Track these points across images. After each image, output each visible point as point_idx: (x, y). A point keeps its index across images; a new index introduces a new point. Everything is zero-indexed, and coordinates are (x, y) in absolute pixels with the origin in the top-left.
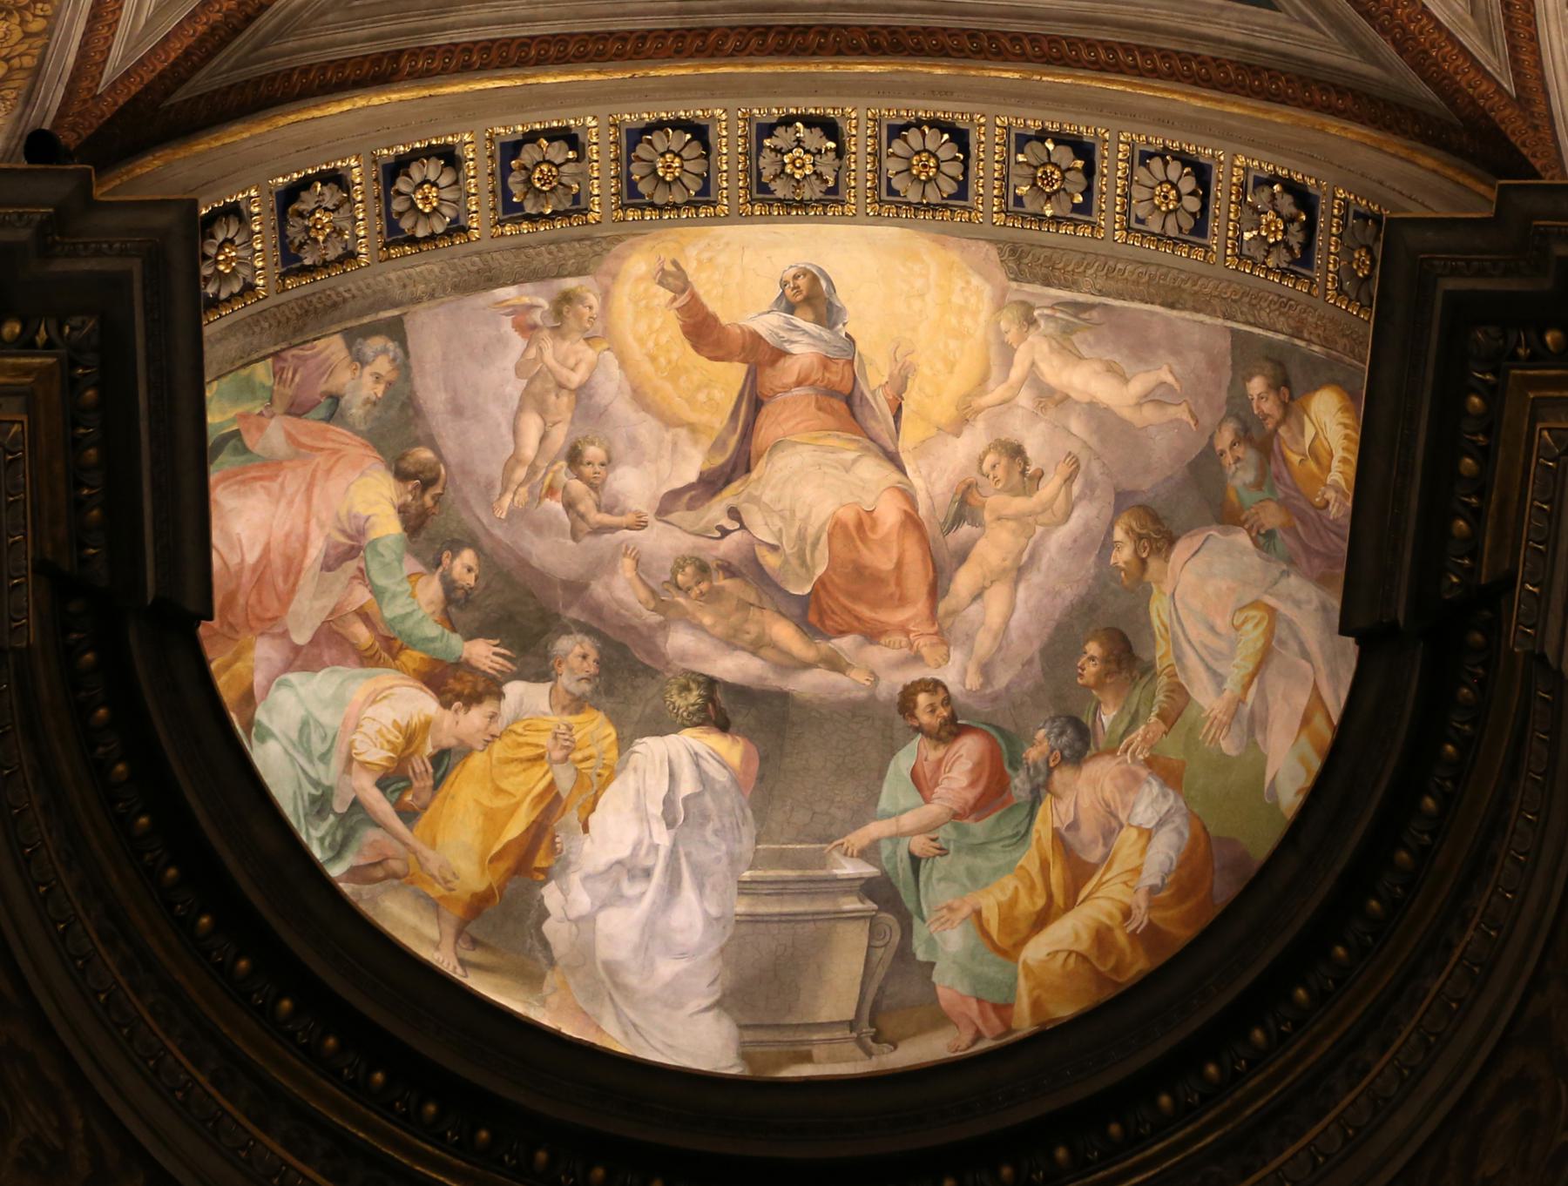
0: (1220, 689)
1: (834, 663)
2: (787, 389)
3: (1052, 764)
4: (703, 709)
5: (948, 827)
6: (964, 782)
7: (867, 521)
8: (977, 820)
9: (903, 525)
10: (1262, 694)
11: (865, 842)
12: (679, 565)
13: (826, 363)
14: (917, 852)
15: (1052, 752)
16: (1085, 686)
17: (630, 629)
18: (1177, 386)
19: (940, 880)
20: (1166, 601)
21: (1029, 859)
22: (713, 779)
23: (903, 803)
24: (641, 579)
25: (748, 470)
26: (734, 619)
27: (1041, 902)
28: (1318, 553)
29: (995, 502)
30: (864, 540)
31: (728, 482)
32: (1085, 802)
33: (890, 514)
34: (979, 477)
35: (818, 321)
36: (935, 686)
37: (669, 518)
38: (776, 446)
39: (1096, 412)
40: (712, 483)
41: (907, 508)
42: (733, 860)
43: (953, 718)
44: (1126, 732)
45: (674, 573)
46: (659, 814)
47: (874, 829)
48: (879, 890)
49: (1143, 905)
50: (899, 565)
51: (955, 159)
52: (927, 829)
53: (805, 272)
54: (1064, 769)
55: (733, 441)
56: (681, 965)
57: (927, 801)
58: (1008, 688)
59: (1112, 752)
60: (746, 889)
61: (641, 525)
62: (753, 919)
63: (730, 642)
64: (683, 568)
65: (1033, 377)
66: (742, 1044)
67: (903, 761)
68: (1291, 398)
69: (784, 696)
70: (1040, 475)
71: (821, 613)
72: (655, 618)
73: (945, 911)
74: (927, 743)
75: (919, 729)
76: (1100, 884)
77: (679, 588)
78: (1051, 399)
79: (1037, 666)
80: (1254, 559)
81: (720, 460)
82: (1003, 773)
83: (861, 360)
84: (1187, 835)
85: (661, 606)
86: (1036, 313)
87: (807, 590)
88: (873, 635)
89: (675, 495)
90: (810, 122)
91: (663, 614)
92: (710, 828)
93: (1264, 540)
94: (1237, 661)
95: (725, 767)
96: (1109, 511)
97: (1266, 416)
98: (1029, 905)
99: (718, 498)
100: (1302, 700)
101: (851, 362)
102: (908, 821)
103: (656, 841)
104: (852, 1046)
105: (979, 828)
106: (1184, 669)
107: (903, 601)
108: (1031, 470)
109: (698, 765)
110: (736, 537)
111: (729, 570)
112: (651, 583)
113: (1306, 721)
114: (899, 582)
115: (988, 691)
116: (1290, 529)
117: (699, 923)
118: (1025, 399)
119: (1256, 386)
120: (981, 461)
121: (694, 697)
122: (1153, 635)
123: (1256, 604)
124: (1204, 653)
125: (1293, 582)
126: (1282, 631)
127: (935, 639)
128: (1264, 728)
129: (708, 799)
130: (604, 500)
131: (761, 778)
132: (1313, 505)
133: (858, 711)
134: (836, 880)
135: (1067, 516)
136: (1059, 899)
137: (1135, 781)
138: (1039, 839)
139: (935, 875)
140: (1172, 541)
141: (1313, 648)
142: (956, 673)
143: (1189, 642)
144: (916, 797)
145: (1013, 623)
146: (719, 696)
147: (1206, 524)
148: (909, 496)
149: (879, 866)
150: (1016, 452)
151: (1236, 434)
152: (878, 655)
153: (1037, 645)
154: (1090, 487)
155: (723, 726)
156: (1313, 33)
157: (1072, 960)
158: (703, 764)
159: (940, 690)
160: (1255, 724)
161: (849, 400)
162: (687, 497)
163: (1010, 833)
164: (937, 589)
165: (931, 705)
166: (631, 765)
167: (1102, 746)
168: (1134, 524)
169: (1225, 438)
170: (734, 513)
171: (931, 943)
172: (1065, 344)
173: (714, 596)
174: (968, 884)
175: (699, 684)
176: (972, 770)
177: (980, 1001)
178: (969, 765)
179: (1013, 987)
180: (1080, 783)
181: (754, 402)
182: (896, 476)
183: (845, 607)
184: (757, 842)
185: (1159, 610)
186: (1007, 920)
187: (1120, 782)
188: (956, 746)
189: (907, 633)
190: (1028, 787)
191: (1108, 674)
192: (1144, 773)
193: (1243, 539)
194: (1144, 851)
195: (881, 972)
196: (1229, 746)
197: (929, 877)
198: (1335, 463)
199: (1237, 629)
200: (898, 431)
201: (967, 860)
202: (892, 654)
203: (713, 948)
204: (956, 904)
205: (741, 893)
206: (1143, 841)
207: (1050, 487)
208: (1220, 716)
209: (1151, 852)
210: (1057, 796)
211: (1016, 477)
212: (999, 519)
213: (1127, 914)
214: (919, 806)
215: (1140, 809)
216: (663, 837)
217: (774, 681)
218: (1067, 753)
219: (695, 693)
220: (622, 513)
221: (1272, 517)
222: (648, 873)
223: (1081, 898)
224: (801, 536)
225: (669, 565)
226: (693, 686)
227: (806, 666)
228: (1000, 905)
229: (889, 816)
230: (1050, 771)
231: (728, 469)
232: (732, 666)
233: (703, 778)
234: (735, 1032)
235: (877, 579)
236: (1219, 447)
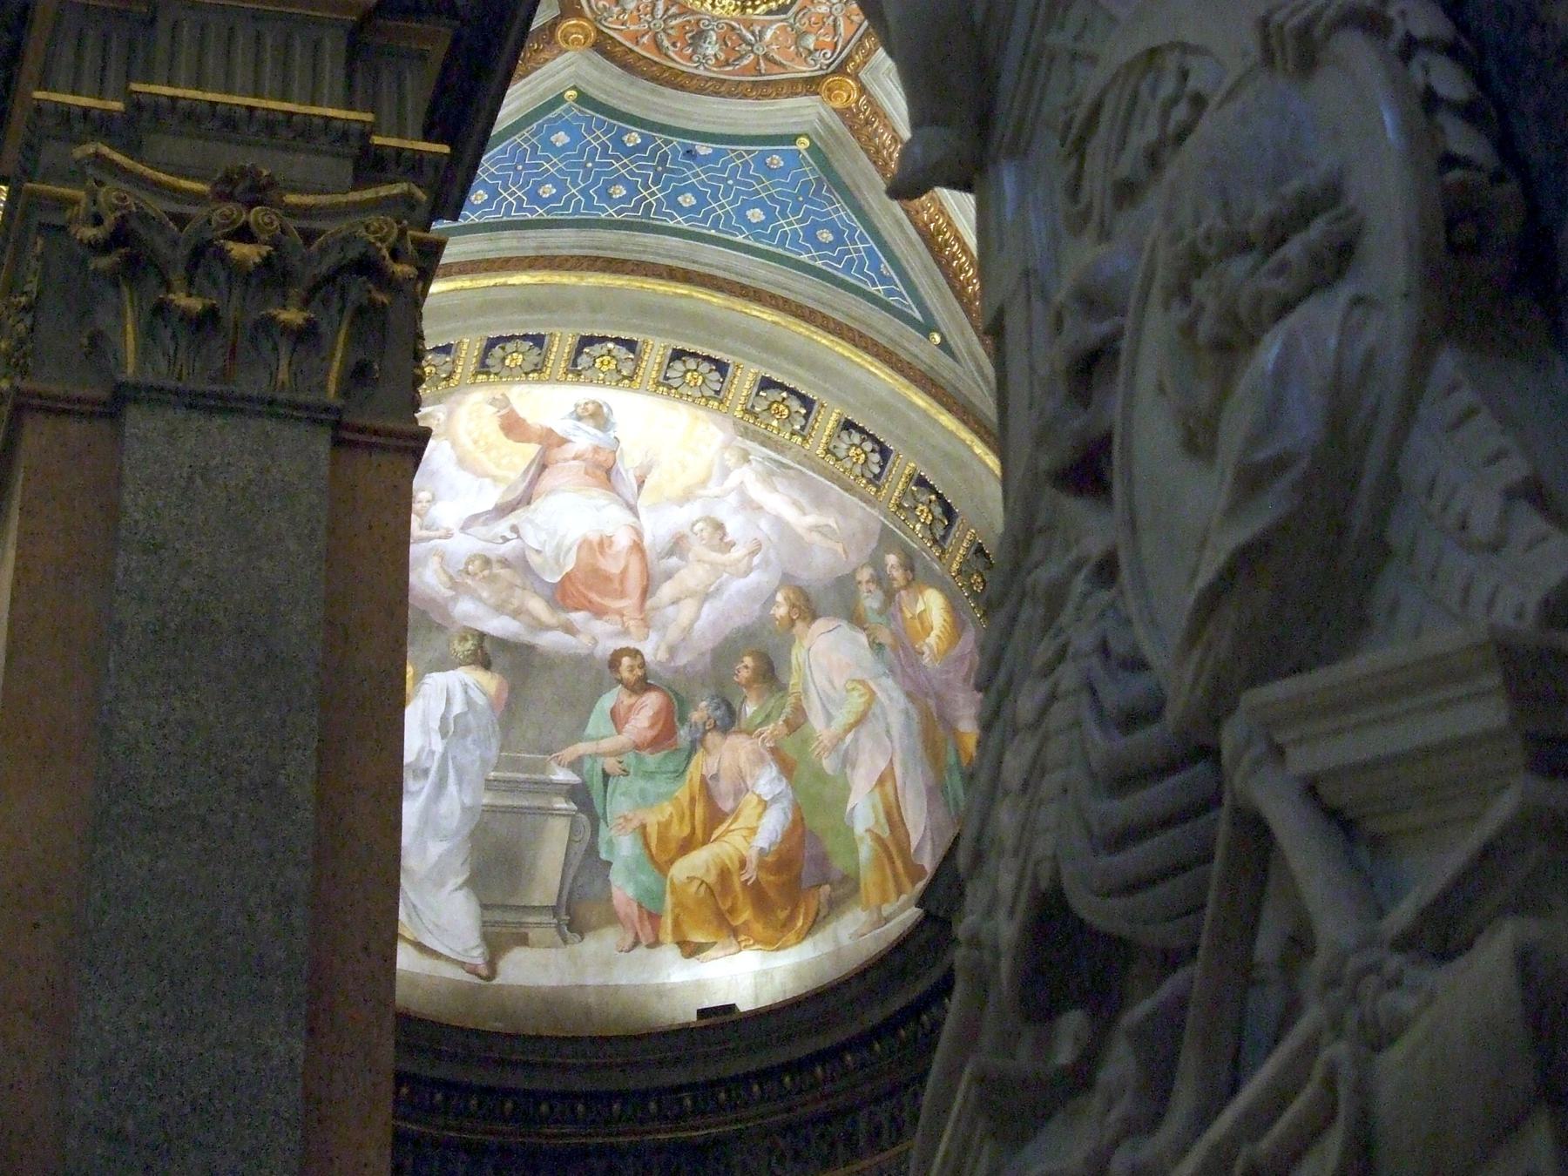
0: (828, 725)
1: (569, 629)
2: (566, 460)
3: (707, 728)
4: (474, 653)
5: (631, 755)
6: (646, 724)
7: (606, 543)
8: (652, 754)
9: (631, 548)
10: (856, 740)
11: (574, 757)
12: (470, 561)
13: (596, 449)
14: (608, 770)
15: (709, 718)
16: (739, 683)
17: (432, 600)
18: (838, 531)
19: (623, 794)
20: (803, 652)
21: (683, 792)
22: (475, 702)
23: (603, 731)
24: (444, 570)
25: (529, 503)
26: (504, 595)
27: (686, 831)
28: (909, 677)
29: (697, 549)
30: (602, 552)
31: (514, 510)
32: (726, 763)
33: (623, 540)
34: (690, 534)
35: (598, 427)
36: (635, 653)
37: (469, 531)
38: (552, 491)
39: (778, 521)
40: (503, 510)
41: (636, 538)
42: (484, 762)
43: (644, 678)
44: (761, 724)
45: (467, 564)
46: (437, 728)
47: (582, 748)
48: (579, 795)
49: (755, 862)
50: (624, 572)
51: (711, 370)
52: (617, 753)
53: (594, 402)
54: (715, 733)
55: (522, 486)
56: (445, 845)
57: (619, 732)
58: (685, 667)
59: (750, 734)
60: (490, 785)
61: (448, 535)
62: (492, 809)
63: (499, 609)
64: (473, 561)
65: (741, 489)
66: (484, 923)
67: (607, 701)
68: (913, 579)
69: (531, 648)
70: (732, 544)
71: (564, 596)
72: (452, 593)
73: (622, 820)
74: (624, 690)
75: (620, 681)
76: (728, 831)
77: (468, 573)
78: (750, 506)
79: (708, 658)
80: (867, 655)
81: (510, 497)
82: (674, 726)
83: (622, 454)
84: (790, 816)
85: (454, 585)
86: (751, 457)
87: (559, 579)
88: (599, 612)
89: (476, 517)
90: (617, 341)
91: (455, 590)
92: (470, 739)
93: (877, 647)
94: (844, 711)
95: (485, 694)
96: (777, 583)
97: (894, 579)
98: (679, 831)
99: (502, 521)
100: (882, 765)
101: (615, 452)
102: (606, 745)
103: (434, 748)
104: (553, 931)
105: (652, 760)
106: (807, 697)
107: (622, 594)
108: (727, 539)
109: (466, 692)
110: (513, 543)
111: (505, 562)
112: (451, 571)
113: (881, 781)
114: (622, 582)
115: (672, 664)
116: (894, 649)
117: (458, 812)
118: (733, 499)
119: (892, 559)
120: (693, 525)
121: (469, 645)
122: (790, 668)
123: (862, 682)
124: (822, 695)
125: (889, 682)
126: (876, 709)
127: (640, 623)
128: (853, 767)
129: (470, 716)
130: (425, 523)
131: (508, 705)
132: (914, 648)
133: (581, 663)
134: (551, 783)
135: (746, 574)
136: (699, 832)
137: (762, 760)
138: (691, 780)
139: (618, 792)
140: (814, 617)
141: (896, 730)
142: (652, 648)
143: (814, 683)
144: (611, 726)
145: (696, 626)
146: (487, 645)
147: (836, 615)
148: (639, 533)
149: (579, 773)
150: (719, 527)
151: (872, 575)
152: (600, 627)
153: (710, 645)
154: (766, 562)
155: (486, 665)
156: (977, 390)
157: (703, 887)
158: (470, 692)
159: (639, 657)
160: (848, 761)
161: (608, 471)
162: (484, 518)
163: (672, 769)
164: (646, 593)
165: (632, 666)
166: (421, 692)
167: (743, 726)
168: (791, 596)
169: (865, 574)
170: (514, 529)
171: (610, 843)
172: (768, 477)
173: (492, 579)
174: (639, 801)
175: (473, 636)
176: (652, 717)
177: (640, 906)
178: (651, 713)
179: (661, 898)
180: (725, 746)
181: (542, 466)
182: (631, 519)
183: (581, 592)
184: (501, 751)
185: (797, 655)
186: (663, 839)
187: (751, 757)
188: (644, 699)
189: (622, 615)
190: (689, 739)
191: (755, 681)
192: (768, 757)
193: (863, 638)
194: (760, 817)
195: (576, 862)
196: (828, 764)
197: (614, 792)
198: (933, 634)
199: (847, 691)
200: (639, 494)
201: (641, 783)
202: (609, 628)
203: (466, 831)
204: (630, 815)
205: (488, 789)
206: (760, 809)
207: (737, 553)
208: (826, 742)
209: (764, 820)
210: (708, 752)
211: (716, 541)
212: (699, 561)
213: (743, 864)
214: (612, 735)
215: (762, 782)
216: (438, 745)
217: (527, 638)
218: (718, 723)
219: (470, 642)
220: (437, 530)
221: (885, 637)
222: (426, 772)
223: (714, 837)
224: (559, 546)
225: (464, 561)
226: (469, 638)
227: (548, 628)
228: (659, 824)
229: (592, 739)
230: (705, 733)
231: (515, 503)
232: (499, 626)
233: (469, 702)
234: (478, 909)
235: (607, 578)
236: (859, 578)
